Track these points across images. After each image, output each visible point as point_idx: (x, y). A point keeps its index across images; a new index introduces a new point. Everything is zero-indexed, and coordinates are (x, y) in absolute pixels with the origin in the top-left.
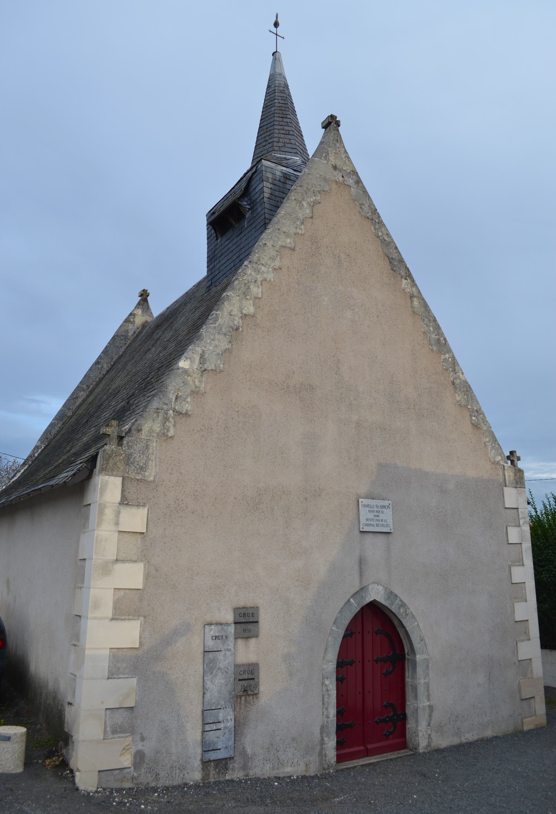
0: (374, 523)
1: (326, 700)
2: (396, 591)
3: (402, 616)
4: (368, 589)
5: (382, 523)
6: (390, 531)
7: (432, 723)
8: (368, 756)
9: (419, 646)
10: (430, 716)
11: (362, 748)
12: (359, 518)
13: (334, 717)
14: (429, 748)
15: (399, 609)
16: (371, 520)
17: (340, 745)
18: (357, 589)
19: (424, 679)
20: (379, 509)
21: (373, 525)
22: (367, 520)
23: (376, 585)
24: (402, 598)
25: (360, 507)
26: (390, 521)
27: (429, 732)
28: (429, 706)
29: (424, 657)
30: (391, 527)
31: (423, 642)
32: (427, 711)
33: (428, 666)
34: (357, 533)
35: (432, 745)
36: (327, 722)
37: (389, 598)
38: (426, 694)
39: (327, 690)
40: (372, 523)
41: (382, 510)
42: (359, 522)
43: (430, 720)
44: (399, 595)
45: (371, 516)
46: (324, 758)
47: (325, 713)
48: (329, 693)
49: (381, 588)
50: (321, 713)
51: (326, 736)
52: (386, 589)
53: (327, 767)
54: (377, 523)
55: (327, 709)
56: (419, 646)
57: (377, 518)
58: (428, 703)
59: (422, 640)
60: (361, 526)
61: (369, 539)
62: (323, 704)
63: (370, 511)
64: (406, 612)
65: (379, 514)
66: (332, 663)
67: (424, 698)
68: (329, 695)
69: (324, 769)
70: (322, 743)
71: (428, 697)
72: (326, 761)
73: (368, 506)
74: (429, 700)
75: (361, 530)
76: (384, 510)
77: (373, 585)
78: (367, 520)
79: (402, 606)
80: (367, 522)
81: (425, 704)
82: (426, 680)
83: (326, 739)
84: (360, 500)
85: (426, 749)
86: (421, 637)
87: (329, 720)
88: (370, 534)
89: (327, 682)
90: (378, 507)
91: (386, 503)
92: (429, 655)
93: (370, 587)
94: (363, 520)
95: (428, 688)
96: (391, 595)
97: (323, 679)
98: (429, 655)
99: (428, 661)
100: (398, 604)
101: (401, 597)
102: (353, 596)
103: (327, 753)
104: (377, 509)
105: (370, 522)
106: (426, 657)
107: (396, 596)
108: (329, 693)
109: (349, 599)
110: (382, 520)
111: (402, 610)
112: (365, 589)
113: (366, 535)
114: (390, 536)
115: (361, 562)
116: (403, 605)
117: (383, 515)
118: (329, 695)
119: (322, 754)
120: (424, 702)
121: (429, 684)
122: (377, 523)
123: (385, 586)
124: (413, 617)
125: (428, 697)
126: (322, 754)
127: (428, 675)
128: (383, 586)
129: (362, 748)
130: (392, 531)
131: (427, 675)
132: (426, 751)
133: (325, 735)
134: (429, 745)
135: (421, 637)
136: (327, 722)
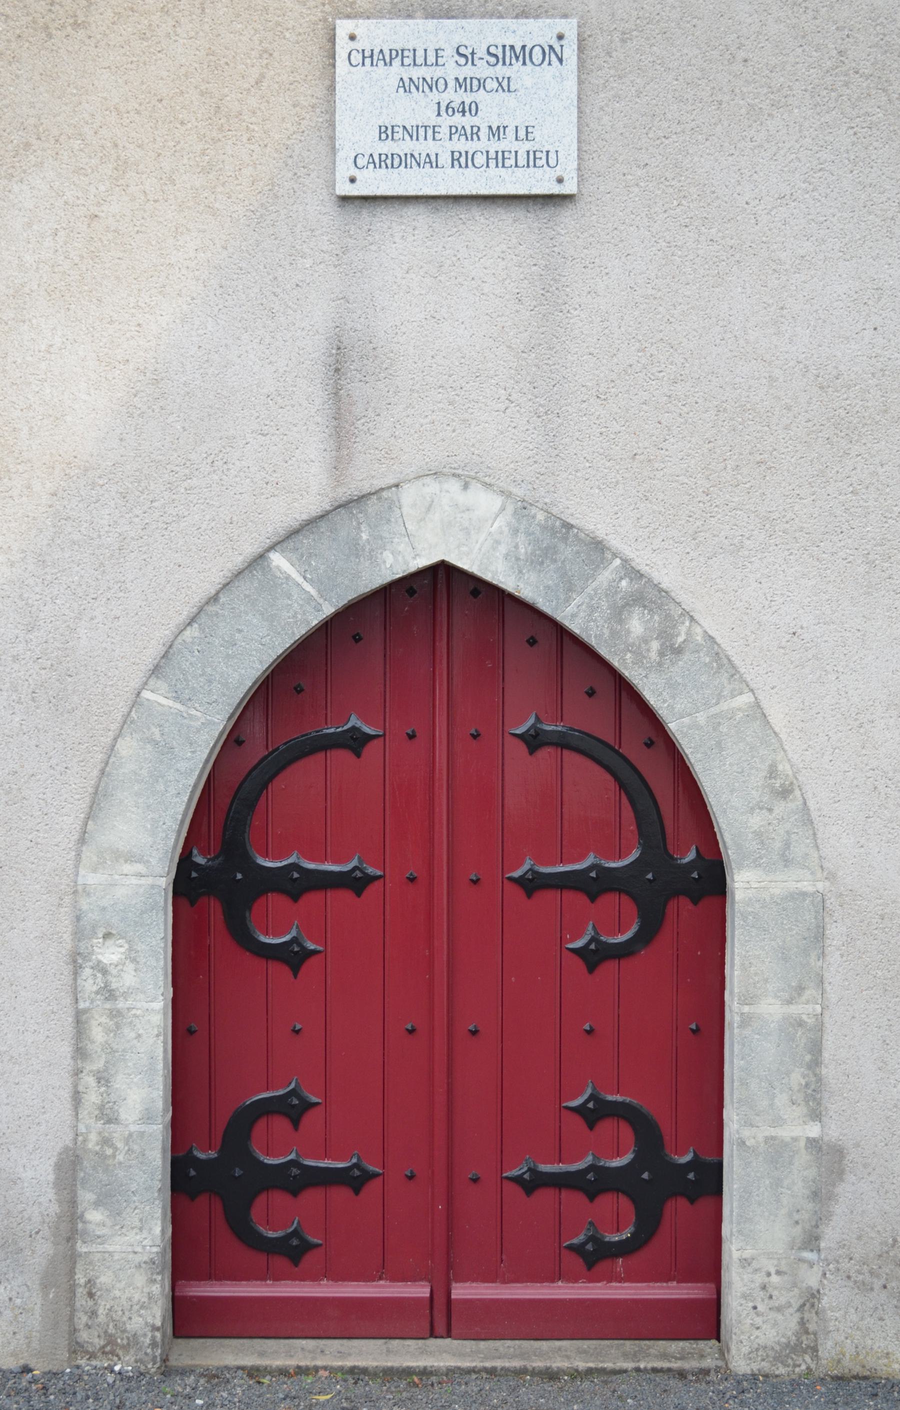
0: (444, 149)
1: (97, 1034)
2: (594, 521)
3: (640, 656)
4: (393, 505)
5: (494, 146)
6: (556, 189)
7: (830, 1236)
8: (449, 1335)
9: (756, 821)
10: (821, 1195)
11: (421, 1291)
12: (332, 125)
13: (147, 1118)
14: (805, 1362)
15: (619, 614)
16: (412, 133)
17: (186, 1256)
18: (311, 504)
19: (789, 1002)
20: (482, 70)
21: (432, 162)
22: (386, 132)
23: (454, 486)
24: (641, 560)
25: (341, 65)
26: (558, 132)
27: (812, 1279)
28: (813, 1143)
29: (792, 886)
30: (568, 167)
31: (793, 804)
32: (801, 1173)
33: (819, 935)
34: (317, 209)
35: (827, 1349)
36: (106, 1141)
37: (542, 556)
38: (797, 1078)
39: (109, 993)
40: (421, 147)
41: (500, 70)
42: (333, 150)
43: (820, 1219)
44: (614, 542)
45: (419, 109)
46: (81, 1300)
47: (92, 1098)
48: (121, 1004)
49: (485, 502)
50: (66, 1094)
51: (97, 1204)
52: (524, 507)
53: (99, 1342)
54: (461, 145)
55: (103, 1079)
56: (756, 821)
57: (458, 120)
58: (813, 1130)
59: (785, 793)
60: (344, 170)
61: (404, 240)
62: (80, 1052)
63: (405, 86)
64: (665, 635)
65: (480, 96)
66: (140, 868)
67: (781, 1099)
68: (116, 1014)
69: (76, 1348)
70: (70, 1228)
71: (814, 1102)
72: (93, 1314)
73: (389, 57)
74: (816, 1115)
75: (345, 189)
76: (516, 71)
77: (431, 487)
78: (386, 132)
79: (637, 599)
80: (387, 147)
81: (785, 1133)
82: (805, 1009)
83: (95, 1216)
84: (344, 27)
85: (779, 1358)
86: (772, 772)
87: (117, 1133)
88: (411, 211)
89: (111, 954)
90: (469, 58)
91: (536, 32)
92: (831, 877)
93: (409, 496)
94: (355, 134)
95: (816, 1048)
96: (559, 538)
97: (79, 934)
98: (831, 877)
99: (821, 903)
100: (612, 590)
101: (629, 553)
102: (288, 538)
103: (104, 1279)
104: (468, 71)
105: (405, 146)
106: (806, 886)
107: (598, 547)
108: (121, 1004)
109: (261, 558)
110: (497, 132)
111: (636, 625)
112: (372, 506)
113: (384, 221)
114: (566, 216)
115: (341, 363)
116: (646, 594)
117: (510, 100)
118: (116, 1014)
119: (66, 1277)
120: (778, 1122)
121: (820, 1028)
122: (461, 145)
123: (518, 491)
124: (720, 661)
125: (814, 1102)
126: (66, 1277)
127: (821, 981)
128: (506, 494)
129: (421, 1291)
130: (570, 188)
131: (807, 981)
132: (781, 1370)
133: (86, 1197)
134: (805, 1341)
135: (772, 772)
136: (106, 1141)
